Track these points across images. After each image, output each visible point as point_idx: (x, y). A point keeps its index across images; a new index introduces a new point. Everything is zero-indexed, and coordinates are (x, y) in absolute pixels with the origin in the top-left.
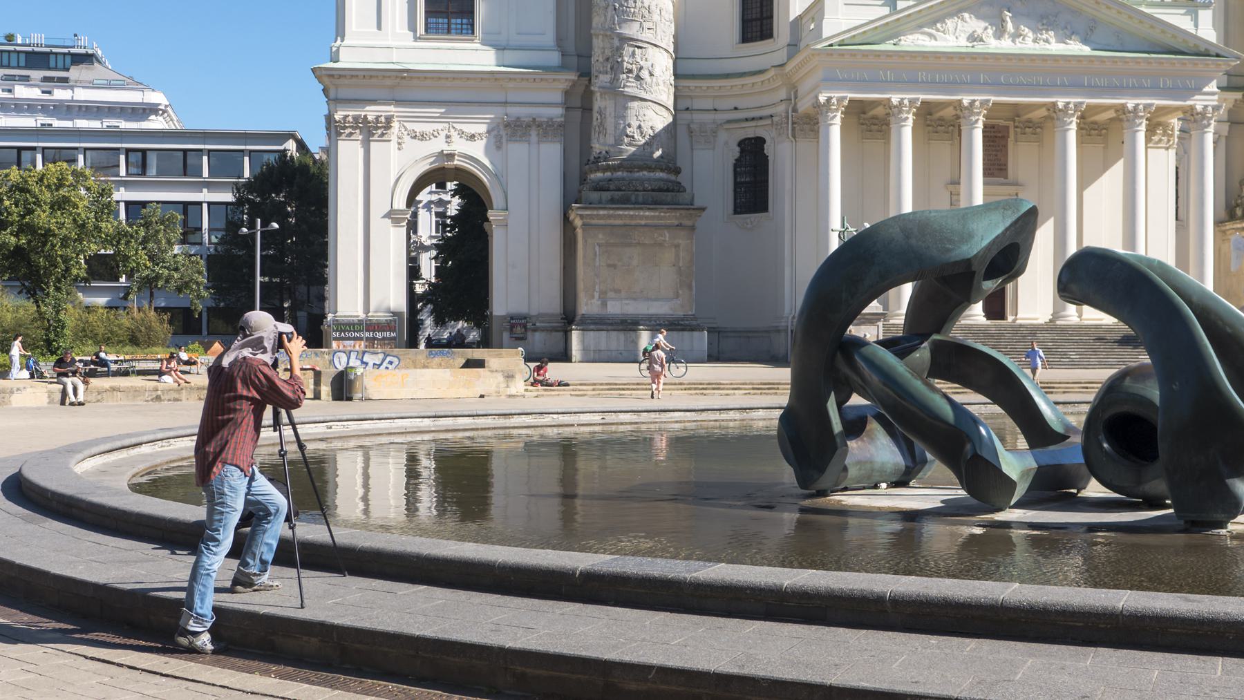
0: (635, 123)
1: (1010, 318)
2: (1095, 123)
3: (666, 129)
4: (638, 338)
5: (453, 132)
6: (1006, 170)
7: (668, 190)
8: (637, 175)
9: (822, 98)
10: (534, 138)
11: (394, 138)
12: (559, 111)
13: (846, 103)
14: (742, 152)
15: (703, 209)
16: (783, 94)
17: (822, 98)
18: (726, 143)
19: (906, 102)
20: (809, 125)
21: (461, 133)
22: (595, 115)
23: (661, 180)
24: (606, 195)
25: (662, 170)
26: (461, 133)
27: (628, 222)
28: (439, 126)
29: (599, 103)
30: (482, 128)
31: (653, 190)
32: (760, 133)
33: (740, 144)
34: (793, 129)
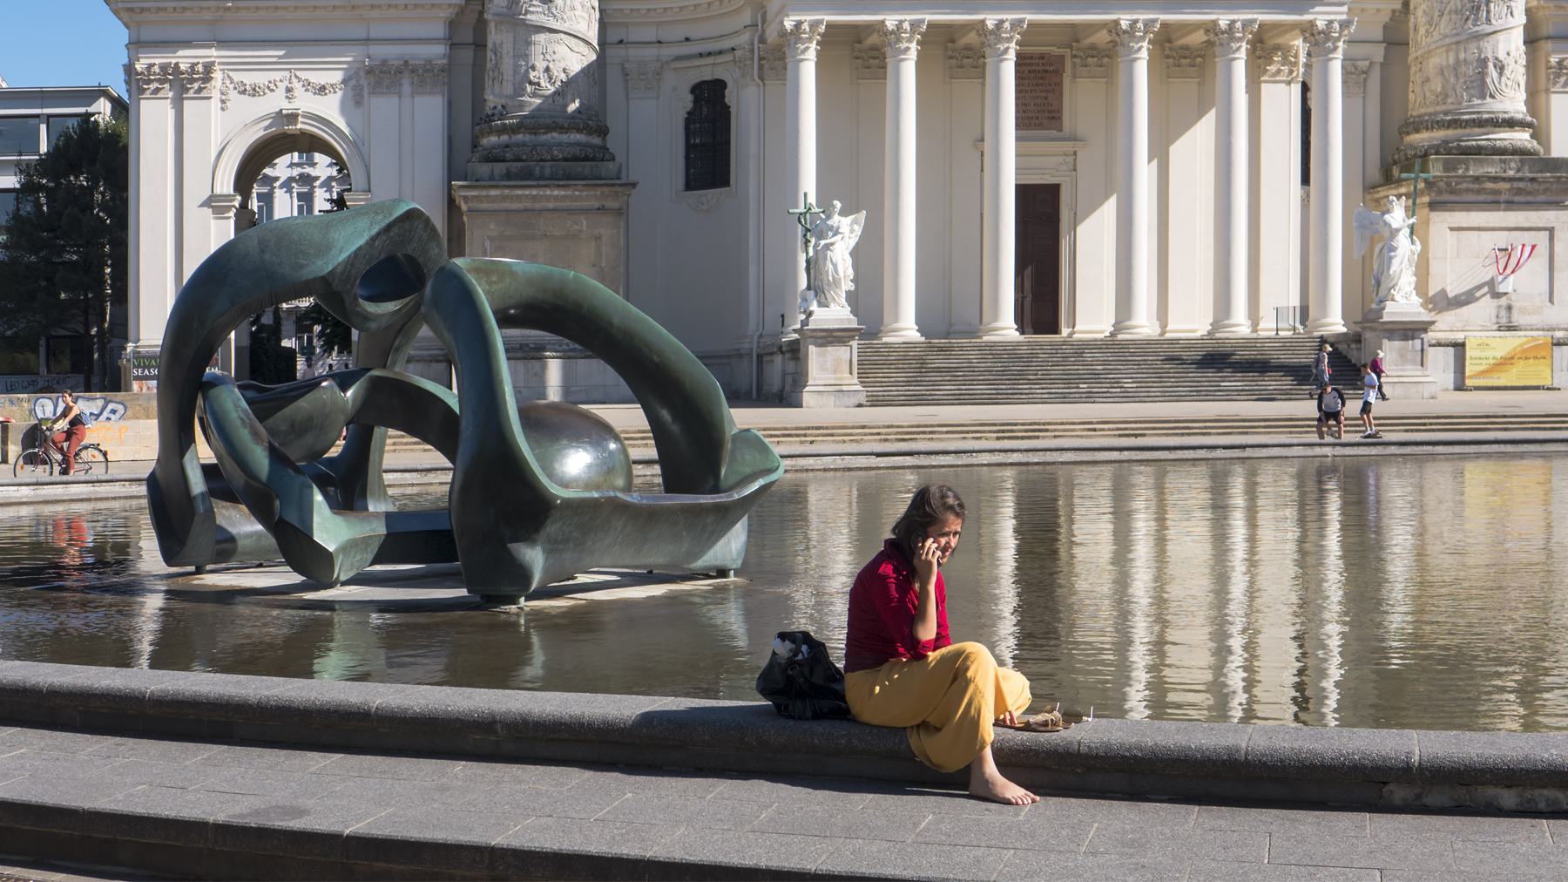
0: (541, 65)
1: (1065, 332)
2: (1186, 48)
3: (586, 71)
4: (544, 368)
5: (297, 85)
6: (1060, 118)
7: (586, 159)
8: (543, 138)
9: (789, 24)
10: (406, 88)
11: (216, 95)
12: (440, 50)
13: (822, 29)
14: (696, 101)
15: (634, 185)
16: (746, 17)
17: (789, 24)
18: (675, 89)
19: (906, 26)
20: (774, 60)
21: (307, 85)
22: (489, 54)
23: (578, 144)
24: (500, 168)
25: (579, 131)
26: (307, 85)
27: (529, 205)
28: (277, 76)
29: (494, 37)
30: (336, 77)
31: (565, 160)
32: (719, 74)
33: (693, 90)
34: (761, 68)
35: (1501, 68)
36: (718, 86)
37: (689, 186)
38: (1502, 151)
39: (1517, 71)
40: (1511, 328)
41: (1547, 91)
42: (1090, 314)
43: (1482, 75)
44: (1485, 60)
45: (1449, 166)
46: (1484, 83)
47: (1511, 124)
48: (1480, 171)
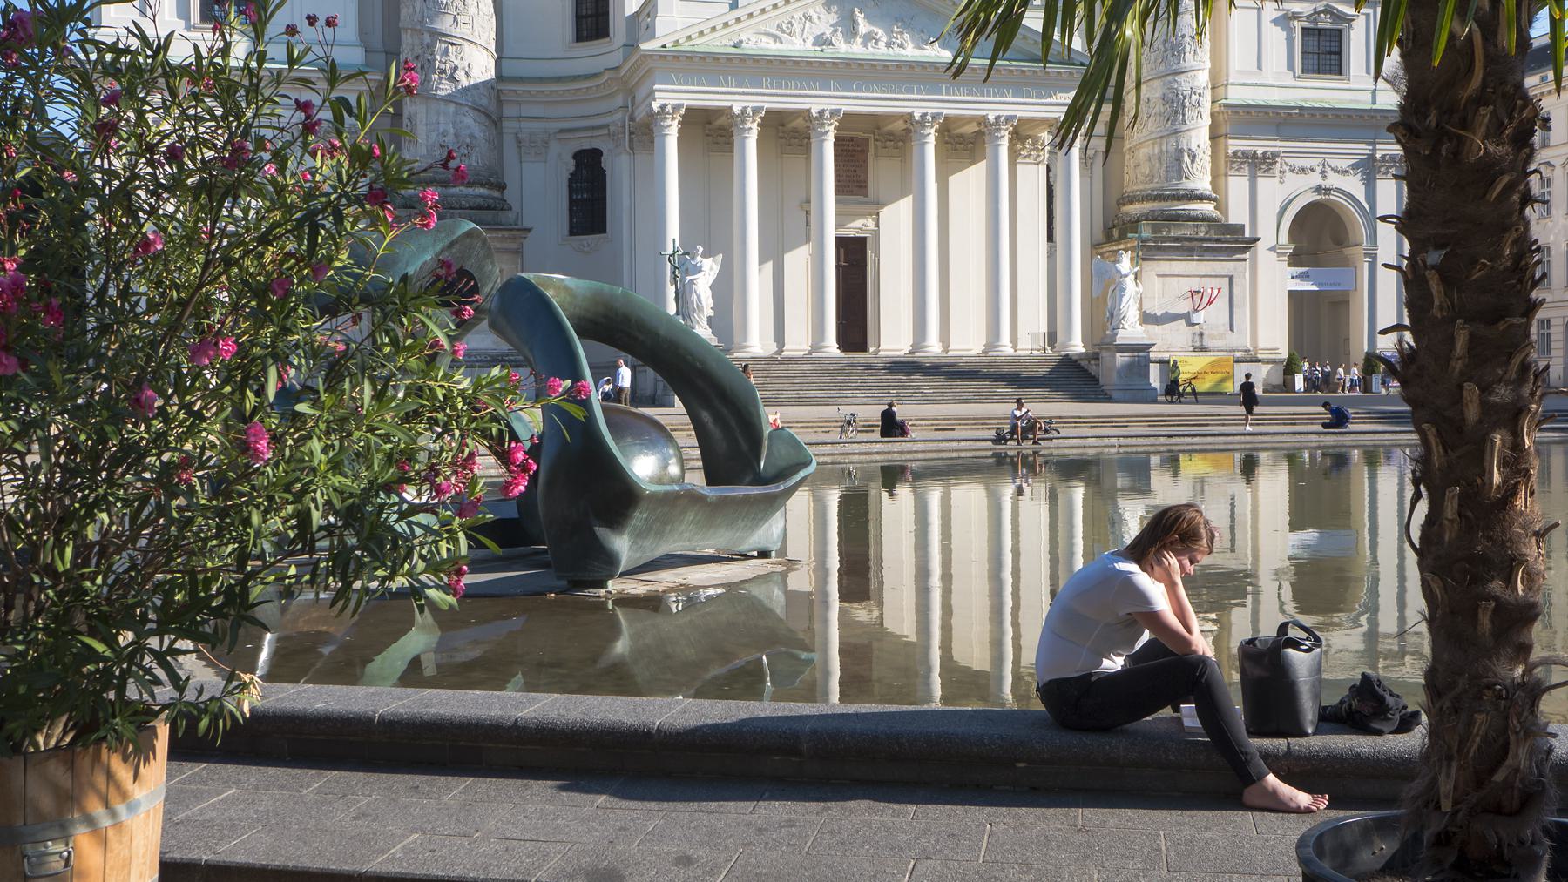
2: (961, 136)
7: (489, 208)
8: (453, 190)
9: (656, 106)
13: (683, 111)
14: (577, 165)
15: (529, 230)
16: (619, 101)
18: (559, 155)
19: (749, 111)
20: (644, 133)
22: (405, 121)
23: (481, 196)
25: (482, 185)
32: (596, 144)
33: (575, 157)
34: (631, 140)
35: (1193, 157)
36: (596, 154)
37: (572, 233)
38: (1195, 219)
39: (1204, 159)
40: (1203, 350)
41: (1226, 175)
42: (893, 335)
43: (1179, 160)
44: (1182, 151)
45: (1155, 230)
46: (1180, 168)
47: (1201, 198)
48: (1179, 233)
